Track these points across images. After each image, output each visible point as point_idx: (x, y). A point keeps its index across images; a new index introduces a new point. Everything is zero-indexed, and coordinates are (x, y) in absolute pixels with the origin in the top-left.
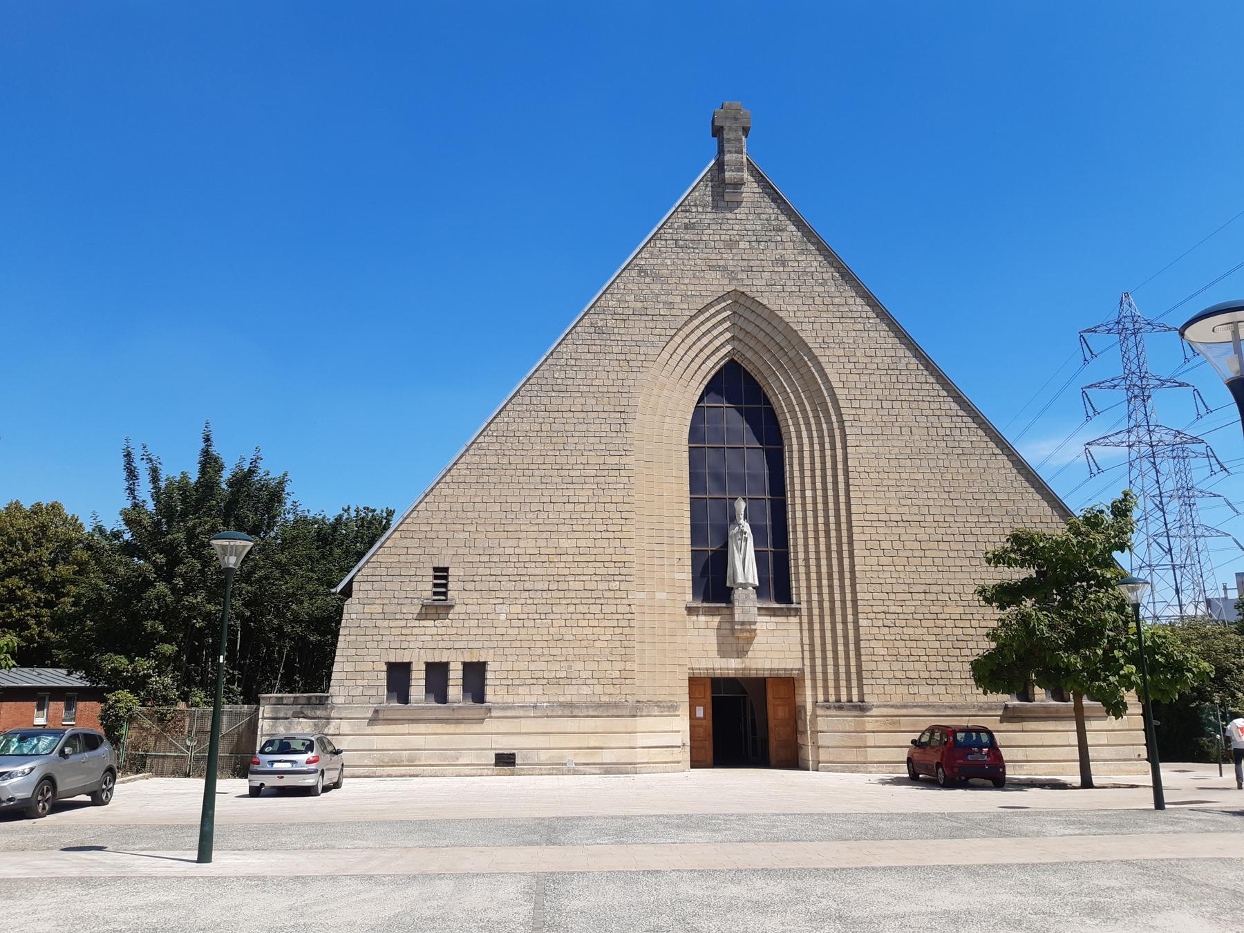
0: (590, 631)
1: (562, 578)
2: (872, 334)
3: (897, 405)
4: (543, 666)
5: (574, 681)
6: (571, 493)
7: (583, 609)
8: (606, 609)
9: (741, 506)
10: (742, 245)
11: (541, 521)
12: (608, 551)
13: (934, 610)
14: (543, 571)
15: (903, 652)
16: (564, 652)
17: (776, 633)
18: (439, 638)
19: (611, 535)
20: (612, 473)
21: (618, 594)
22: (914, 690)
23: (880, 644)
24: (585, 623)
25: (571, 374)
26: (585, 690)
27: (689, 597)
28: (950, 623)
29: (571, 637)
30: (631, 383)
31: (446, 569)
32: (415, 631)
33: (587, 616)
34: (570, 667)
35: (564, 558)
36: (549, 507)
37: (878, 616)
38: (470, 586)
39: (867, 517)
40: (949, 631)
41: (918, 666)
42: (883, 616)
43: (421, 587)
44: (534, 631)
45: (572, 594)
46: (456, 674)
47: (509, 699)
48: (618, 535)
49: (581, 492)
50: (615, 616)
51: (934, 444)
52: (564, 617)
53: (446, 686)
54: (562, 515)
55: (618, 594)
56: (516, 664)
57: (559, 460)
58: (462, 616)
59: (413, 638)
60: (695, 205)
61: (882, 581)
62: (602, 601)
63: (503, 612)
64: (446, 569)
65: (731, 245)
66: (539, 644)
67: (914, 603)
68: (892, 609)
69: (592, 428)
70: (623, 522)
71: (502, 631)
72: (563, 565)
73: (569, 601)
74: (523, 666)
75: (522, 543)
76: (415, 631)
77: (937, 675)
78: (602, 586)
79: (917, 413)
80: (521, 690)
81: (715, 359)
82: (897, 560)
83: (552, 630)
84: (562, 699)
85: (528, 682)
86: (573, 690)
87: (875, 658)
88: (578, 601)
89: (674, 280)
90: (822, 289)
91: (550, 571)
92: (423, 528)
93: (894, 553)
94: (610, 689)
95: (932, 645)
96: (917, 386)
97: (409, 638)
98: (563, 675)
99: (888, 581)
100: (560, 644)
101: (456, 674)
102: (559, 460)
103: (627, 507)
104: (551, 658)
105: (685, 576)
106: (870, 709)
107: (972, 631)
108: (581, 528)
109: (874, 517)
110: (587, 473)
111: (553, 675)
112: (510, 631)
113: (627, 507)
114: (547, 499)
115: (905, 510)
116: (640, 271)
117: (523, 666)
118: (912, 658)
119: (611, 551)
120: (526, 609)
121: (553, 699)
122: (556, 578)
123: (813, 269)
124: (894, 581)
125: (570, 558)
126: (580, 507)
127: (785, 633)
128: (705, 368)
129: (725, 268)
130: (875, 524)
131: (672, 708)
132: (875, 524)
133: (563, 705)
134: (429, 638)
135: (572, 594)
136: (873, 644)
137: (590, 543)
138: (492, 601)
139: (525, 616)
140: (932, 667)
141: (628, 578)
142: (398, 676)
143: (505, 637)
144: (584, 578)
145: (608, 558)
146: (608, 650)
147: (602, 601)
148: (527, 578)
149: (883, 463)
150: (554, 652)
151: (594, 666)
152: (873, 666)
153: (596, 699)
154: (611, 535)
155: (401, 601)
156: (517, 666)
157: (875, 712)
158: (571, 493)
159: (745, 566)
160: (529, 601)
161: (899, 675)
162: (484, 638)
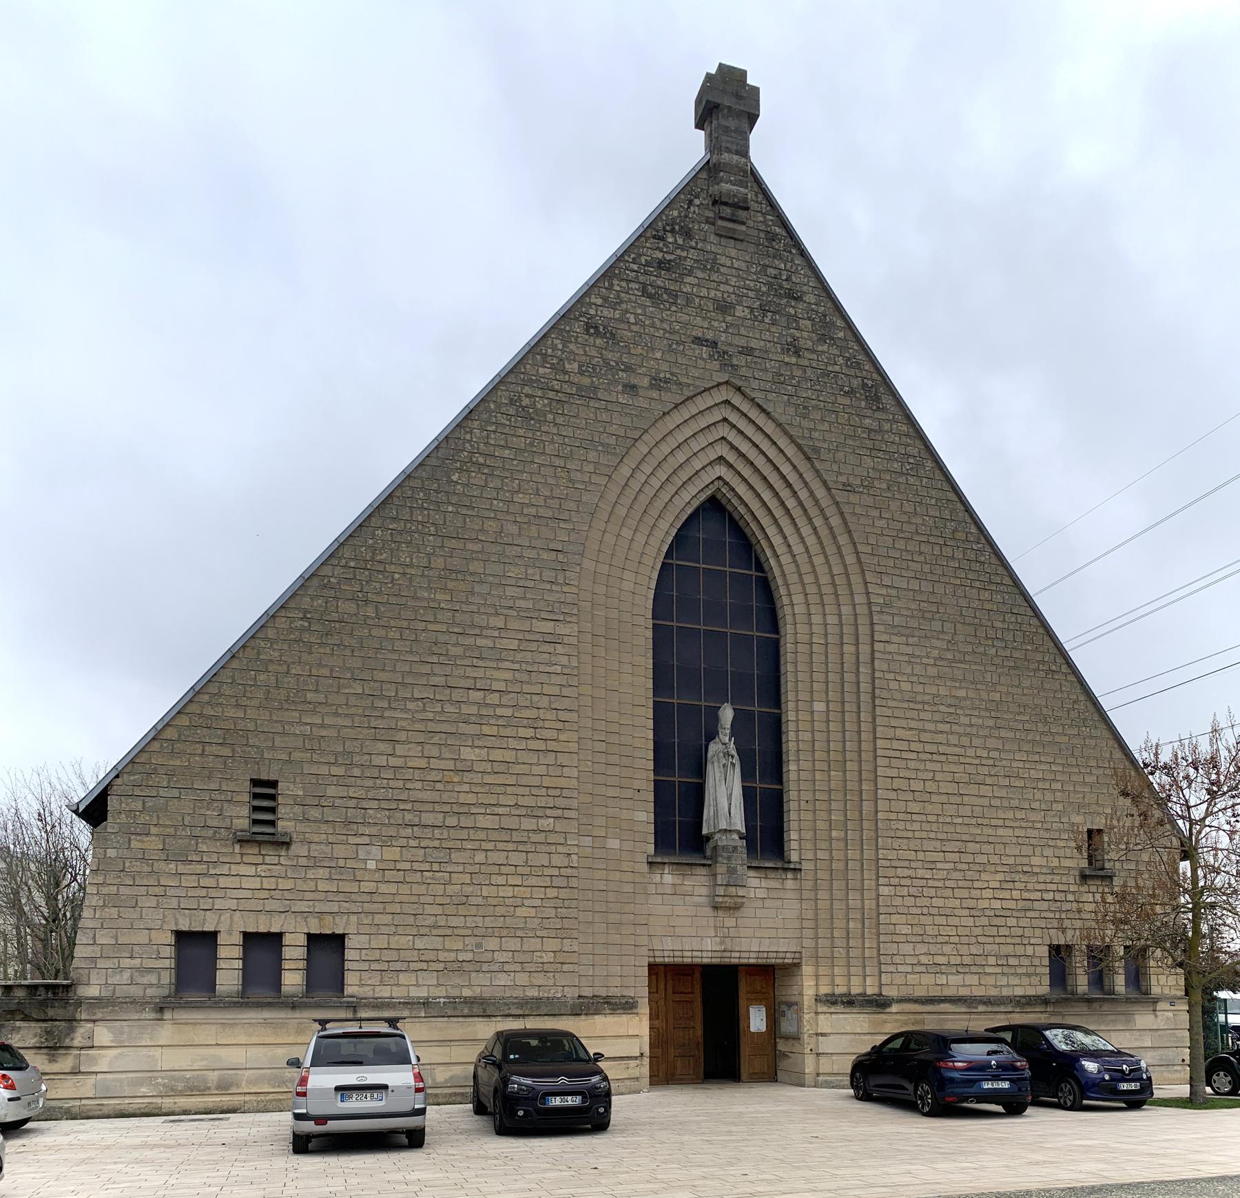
0: (509, 892)
1: (465, 809)
2: (911, 480)
3: (939, 589)
4: (437, 943)
5: (485, 967)
6: (479, 673)
7: (499, 858)
8: (536, 860)
9: (727, 714)
10: (739, 311)
11: (431, 716)
12: (537, 770)
13: (969, 875)
14: (434, 796)
15: (929, 930)
16: (470, 922)
17: (768, 903)
18: (265, 894)
19: (540, 745)
20: (546, 648)
21: (552, 838)
22: (942, 980)
23: (903, 919)
24: (501, 880)
25: (478, 479)
26: (503, 979)
27: (651, 849)
28: (988, 893)
29: (480, 901)
30: (573, 506)
31: (273, 784)
32: (223, 882)
33: (504, 870)
34: (479, 946)
35: (468, 777)
36: (443, 694)
37: (903, 882)
38: (314, 813)
39: (896, 744)
40: (985, 904)
41: (947, 949)
42: (908, 882)
43: (230, 810)
44: (422, 889)
45: (482, 835)
46: (294, 951)
47: (384, 992)
48: (552, 745)
49: (497, 674)
50: (548, 872)
51: (981, 649)
52: (469, 869)
53: (279, 970)
54: (466, 709)
55: (552, 838)
56: (394, 939)
57: (459, 617)
58: (303, 861)
59: (221, 893)
60: (673, 231)
61: (910, 834)
62: (528, 847)
63: (372, 858)
64: (273, 784)
65: (724, 308)
66: (429, 910)
67: (947, 866)
68: (921, 873)
69: (513, 572)
70: (559, 725)
71: (370, 887)
72: (466, 788)
73: (476, 845)
74: (404, 941)
75: (400, 750)
76: (223, 882)
77: (967, 960)
78: (529, 824)
79: (963, 603)
80: (403, 978)
81: (692, 490)
82: (929, 808)
83: (451, 889)
84: (467, 993)
85: (413, 966)
86: (482, 979)
87: (896, 938)
88: (490, 846)
89: (639, 350)
90: (847, 401)
91: (445, 797)
92: (231, 712)
93: (926, 797)
94: (539, 979)
95: (965, 921)
96: (965, 564)
97: (213, 893)
98: (469, 956)
99: (917, 834)
100: (462, 910)
101: (294, 951)
102: (459, 617)
103: (565, 703)
104: (448, 932)
105: (644, 816)
106: (889, 1005)
107: (1012, 904)
108: (494, 731)
109: (904, 746)
110: (505, 643)
111: (452, 956)
112: (384, 888)
113: (565, 703)
114: (439, 680)
115: (941, 738)
116: (588, 326)
117: (404, 941)
118: (940, 939)
119: (541, 770)
120: (407, 855)
121: (455, 993)
122: (456, 808)
123: (837, 368)
124: (924, 835)
125: (477, 778)
126: (493, 698)
127: (779, 903)
128: (679, 502)
129: (714, 344)
130: (904, 755)
131: (626, 1006)
132: (904, 755)
133: (468, 1001)
134: (248, 894)
135: (482, 835)
136: (895, 919)
137: (509, 756)
138: (352, 840)
139: (407, 866)
140: (964, 950)
141: (567, 814)
142: (195, 947)
143: (375, 898)
144: (501, 810)
145: (535, 781)
146: (537, 921)
147: (528, 847)
148: (409, 806)
149: (918, 669)
150: (454, 921)
151: (514, 944)
152: (893, 949)
153: (518, 993)
154: (540, 745)
155: (197, 832)
156: (396, 942)
157: (895, 1008)
158: (479, 673)
159: (725, 801)
160: (413, 843)
161: (924, 960)
162: (341, 897)
